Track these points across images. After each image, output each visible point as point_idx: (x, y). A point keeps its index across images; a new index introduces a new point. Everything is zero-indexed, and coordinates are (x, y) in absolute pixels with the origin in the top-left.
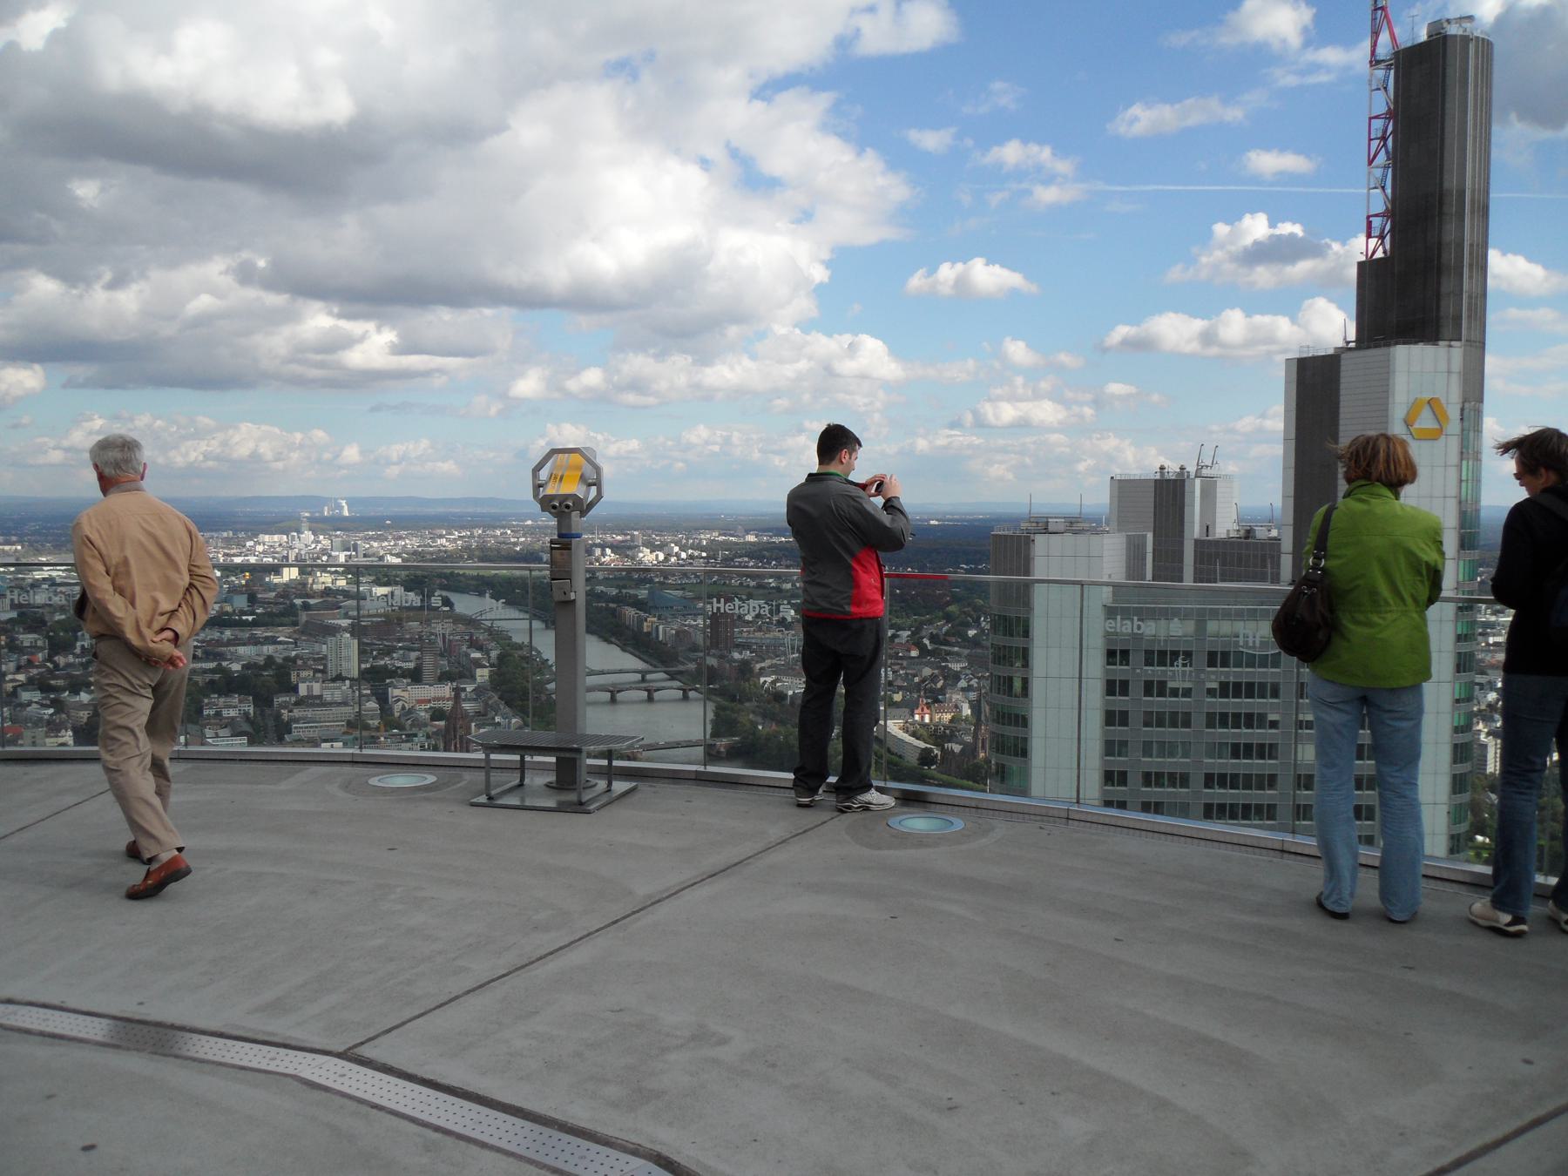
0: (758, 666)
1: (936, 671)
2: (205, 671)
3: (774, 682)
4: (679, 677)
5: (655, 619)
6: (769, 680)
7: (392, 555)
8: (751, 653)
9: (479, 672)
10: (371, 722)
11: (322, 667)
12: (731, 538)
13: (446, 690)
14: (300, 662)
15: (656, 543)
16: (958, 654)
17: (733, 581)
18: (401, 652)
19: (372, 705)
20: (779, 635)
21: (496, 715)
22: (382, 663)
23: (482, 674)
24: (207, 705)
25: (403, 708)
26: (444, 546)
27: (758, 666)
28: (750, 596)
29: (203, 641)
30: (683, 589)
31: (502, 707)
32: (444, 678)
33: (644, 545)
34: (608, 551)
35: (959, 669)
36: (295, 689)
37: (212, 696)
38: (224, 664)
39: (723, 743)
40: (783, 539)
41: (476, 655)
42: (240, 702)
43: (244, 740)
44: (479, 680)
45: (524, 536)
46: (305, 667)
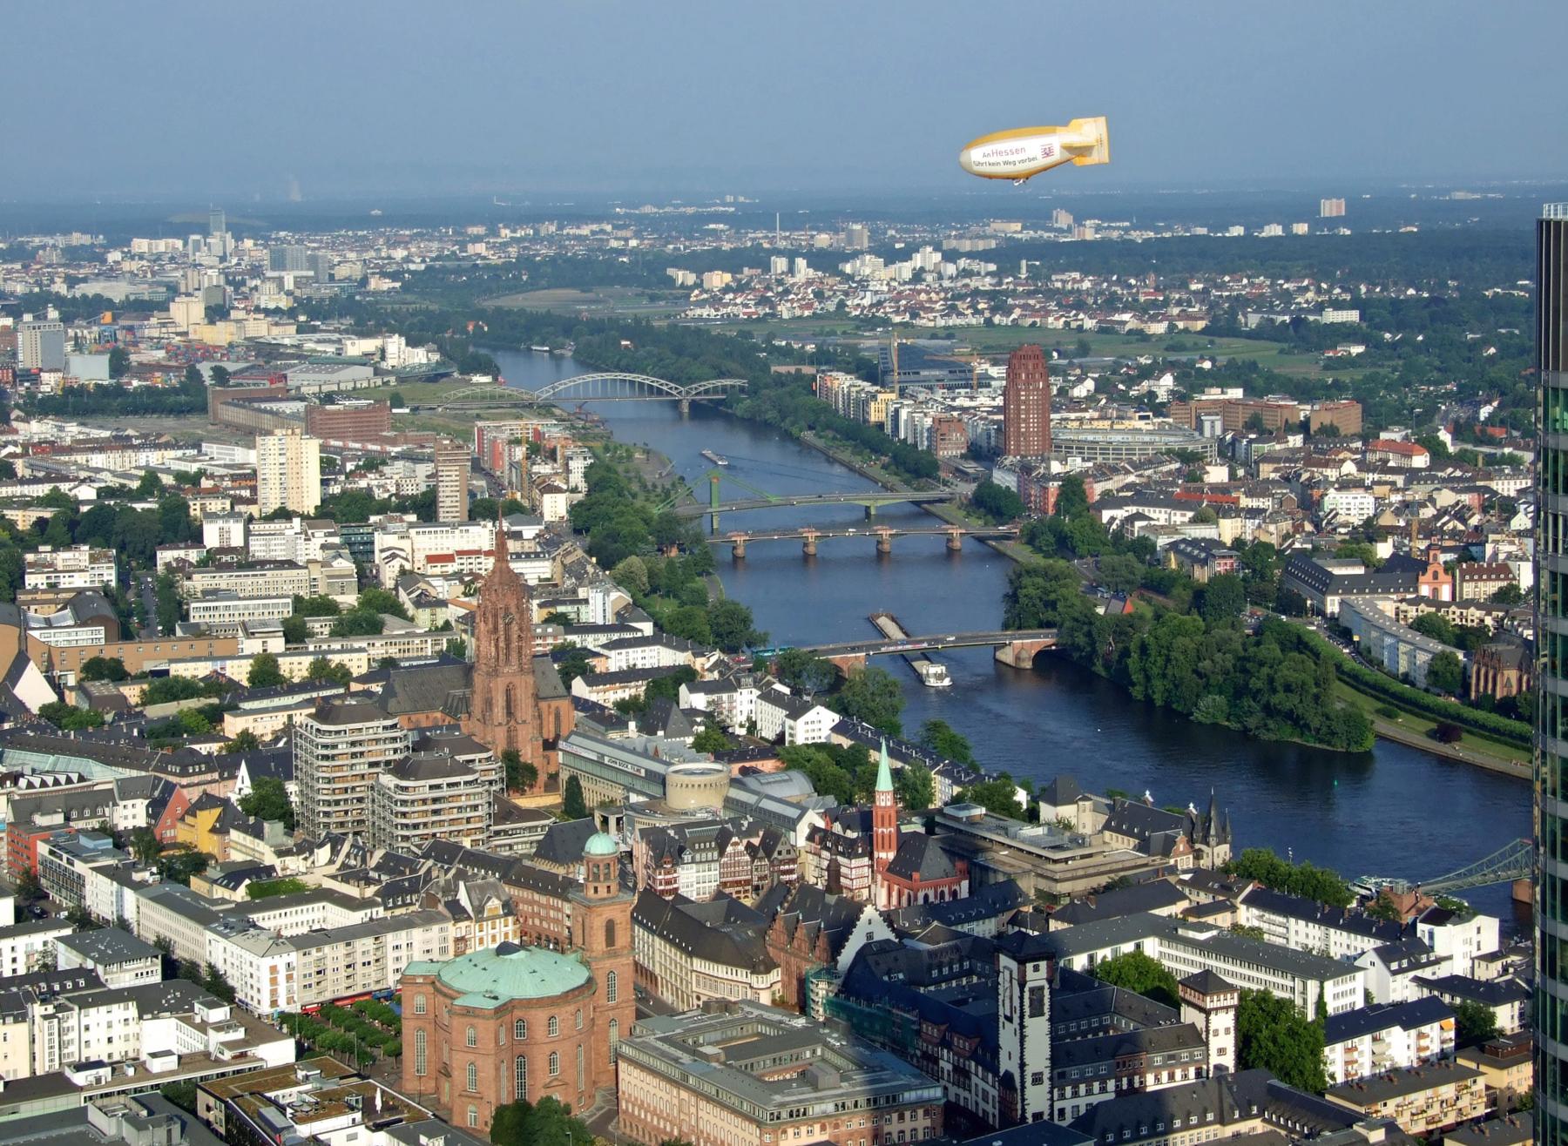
0: (1098, 488)
1: (1466, 498)
2: (26, 504)
3: (1131, 519)
4: (936, 509)
5: (893, 396)
6: (1121, 514)
7: (384, 275)
8: (1083, 460)
9: (548, 499)
10: (339, 598)
11: (246, 493)
12: (1046, 235)
13: (481, 536)
14: (206, 483)
15: (898, 246)
16: (1514, 462)
17: (1050, 319)
18: (400, 464)
19: (345, 565)
20: (1141, 424)
21: (580, 585)
22: (363, 484)
23: (555, 507)
24: (32, 565)
25: (403, 572)
26: (484, 258)
27: (1098, 488)
28: (1084, 350)
29: (25, 446)
30: (949, 337)
31: (590, 569)
32: (479, 511)
33: (871, 251)
34: (801, 263)
35: (1513, 494)
36: (196, 538)
37: (41, 548)
38: (64, 487)
39: (1024, 647)
40: (1152, 234)
41: (543, 469)
42: (93, 559)
43: (100, 632)
44: (548, 517)
45: (637, 235)
46: (214, 493)
